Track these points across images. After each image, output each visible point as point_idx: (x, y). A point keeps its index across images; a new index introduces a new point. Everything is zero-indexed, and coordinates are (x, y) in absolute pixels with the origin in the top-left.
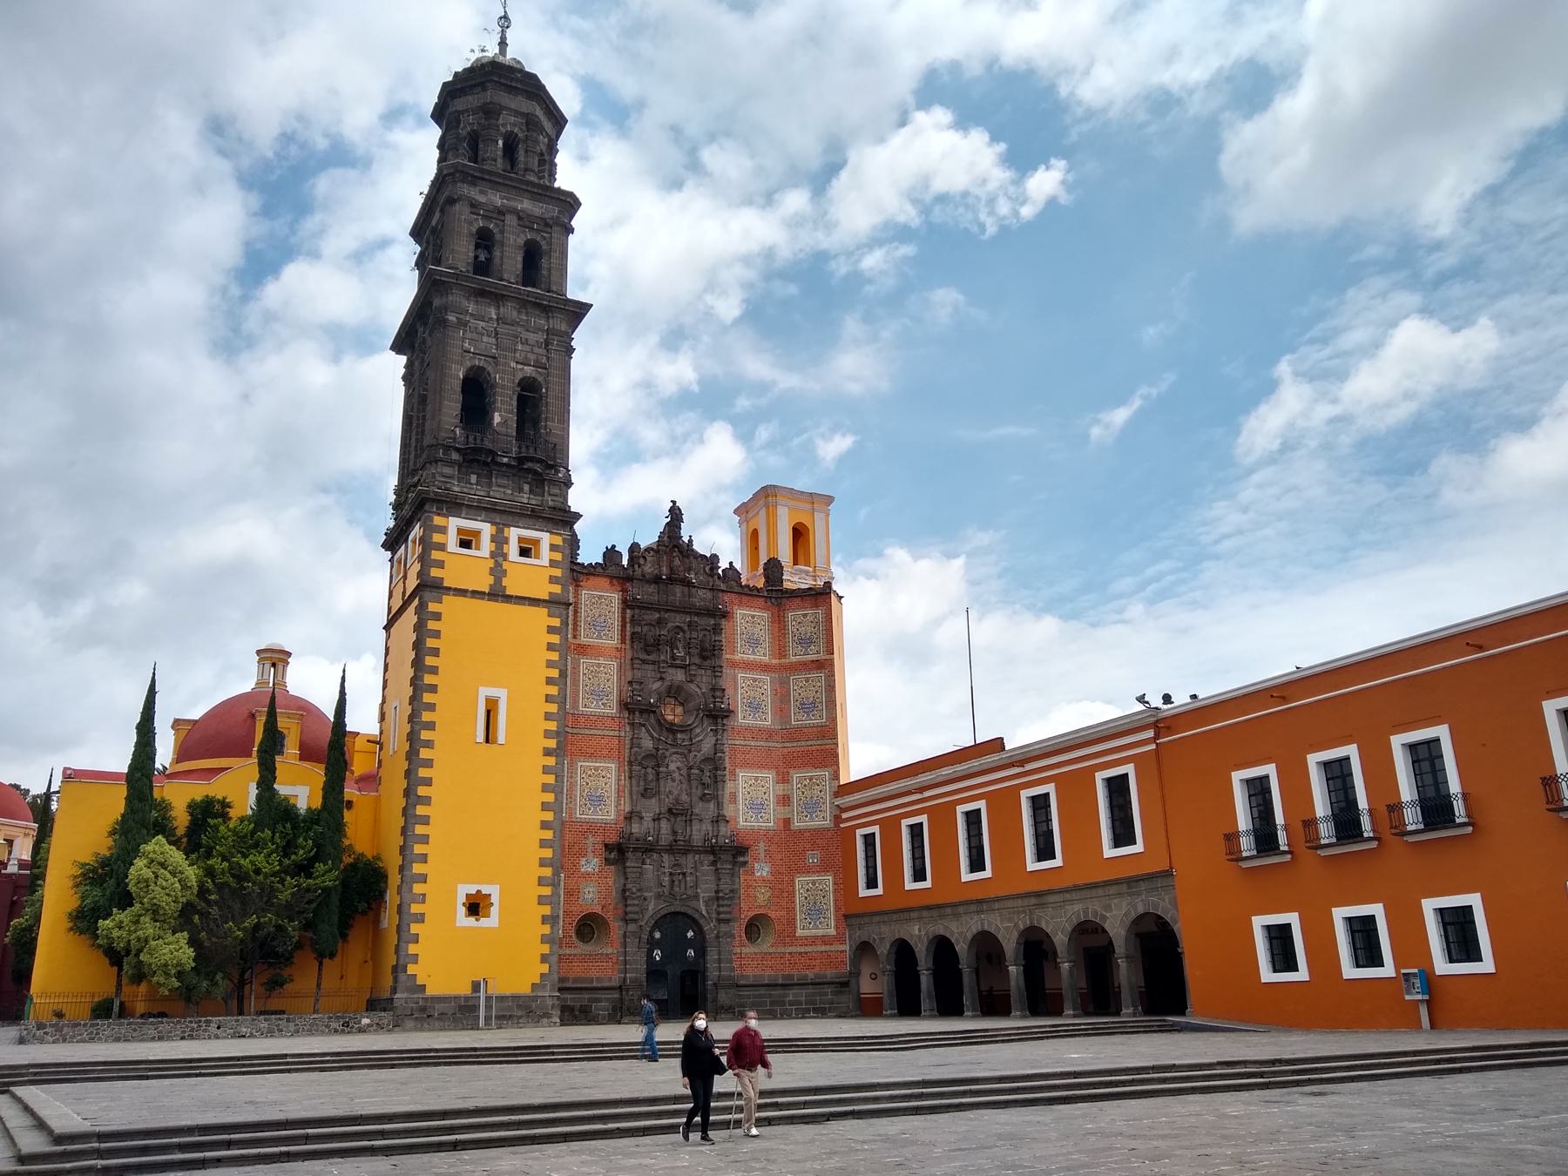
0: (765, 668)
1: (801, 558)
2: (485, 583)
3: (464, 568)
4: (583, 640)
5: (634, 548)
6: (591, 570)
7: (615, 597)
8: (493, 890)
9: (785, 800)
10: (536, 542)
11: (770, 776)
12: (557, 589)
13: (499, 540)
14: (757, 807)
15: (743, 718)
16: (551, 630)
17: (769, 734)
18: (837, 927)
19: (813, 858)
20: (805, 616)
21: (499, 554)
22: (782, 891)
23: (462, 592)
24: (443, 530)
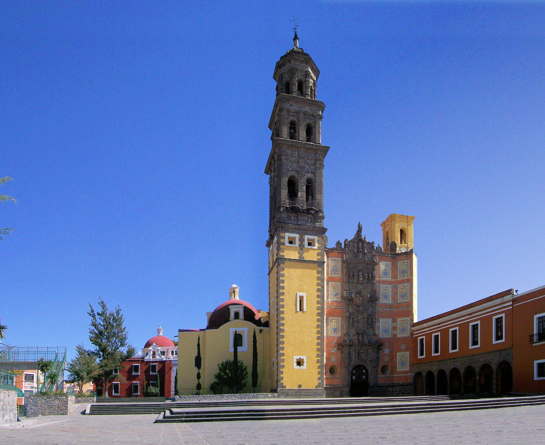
0: (390, 283)
1: (403, 242)
9: (394, 328)
11: (390, 320)
13: (302, 240)
14: (386, 331)
15: (382, 301)
17: (390, 306)
18: (410, 368)
19: (403, 347)
20: (404, 263)
21: (302, 246)
22: (392, 357)
23: (290, 260)
24: (284, 238)
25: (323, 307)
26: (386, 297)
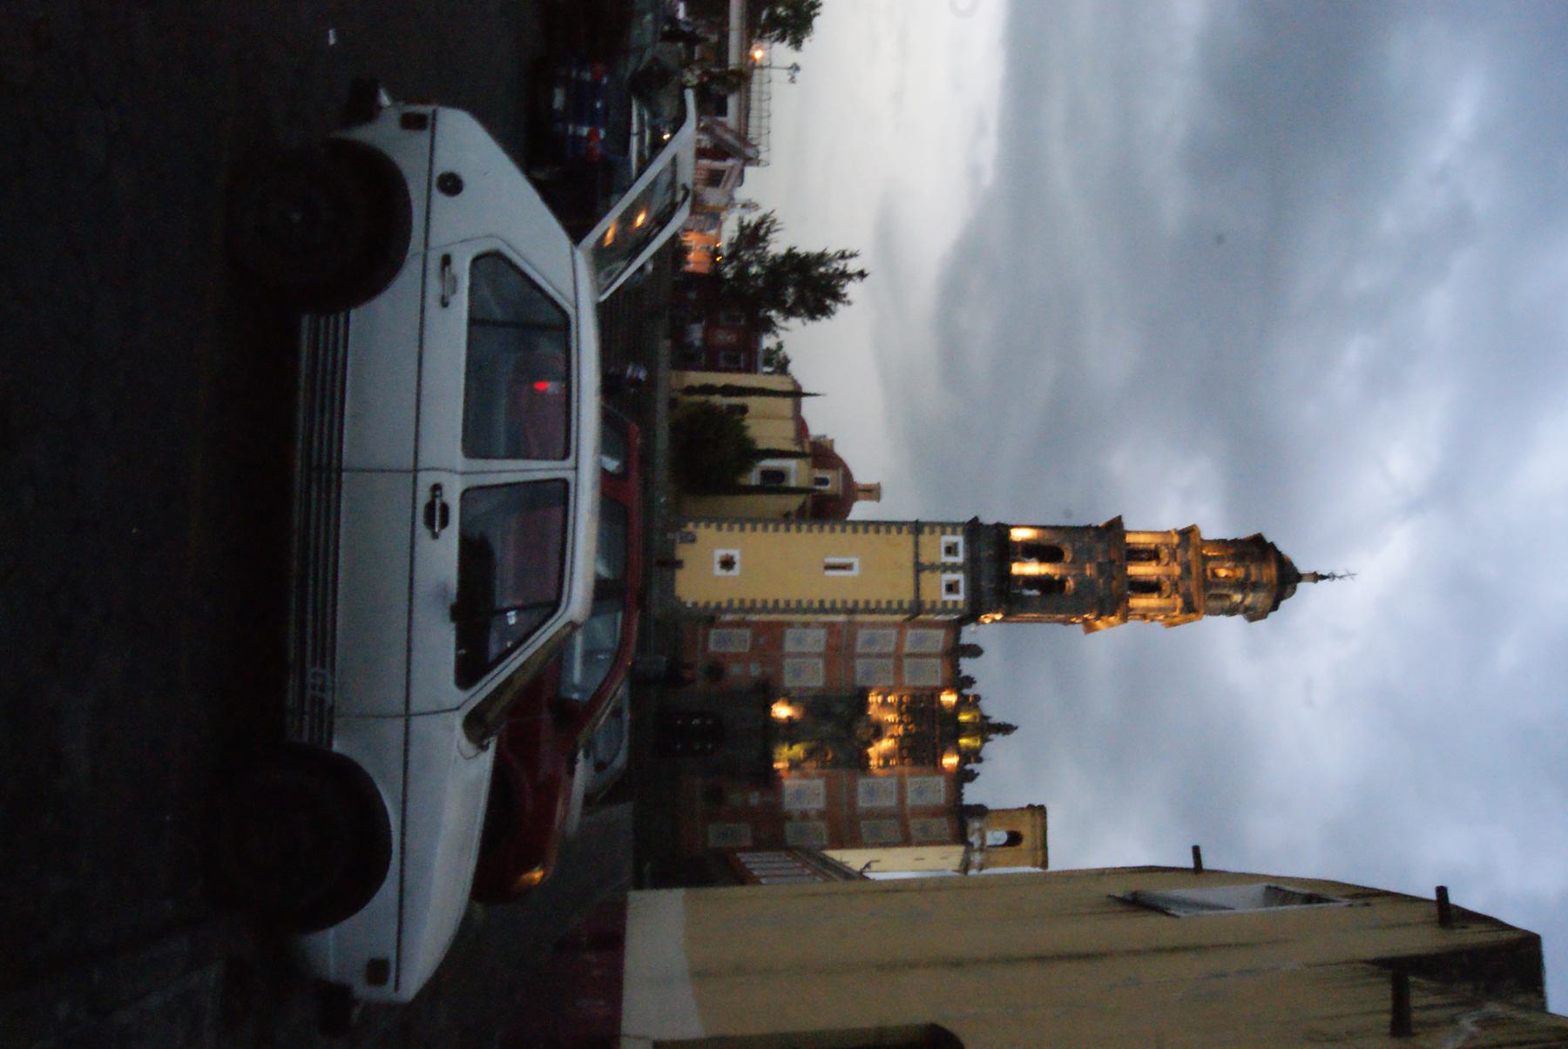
0: (902, 800)
2: (924, 559)
3: (934, 548)
4: (906, 662)
5: (977, 698)
6: (956, 669)
7: (938, 683)
8: (736, 571)
9: (805, 816)
10: (957, 592)
12: (928, 606)
13: (954, 568)
16: (900, 603)
17: (852, 803)
21: (945, 568)
23: (917, 545)
24: (954, 533)
25: (833, 610)
26: (871, 793)
